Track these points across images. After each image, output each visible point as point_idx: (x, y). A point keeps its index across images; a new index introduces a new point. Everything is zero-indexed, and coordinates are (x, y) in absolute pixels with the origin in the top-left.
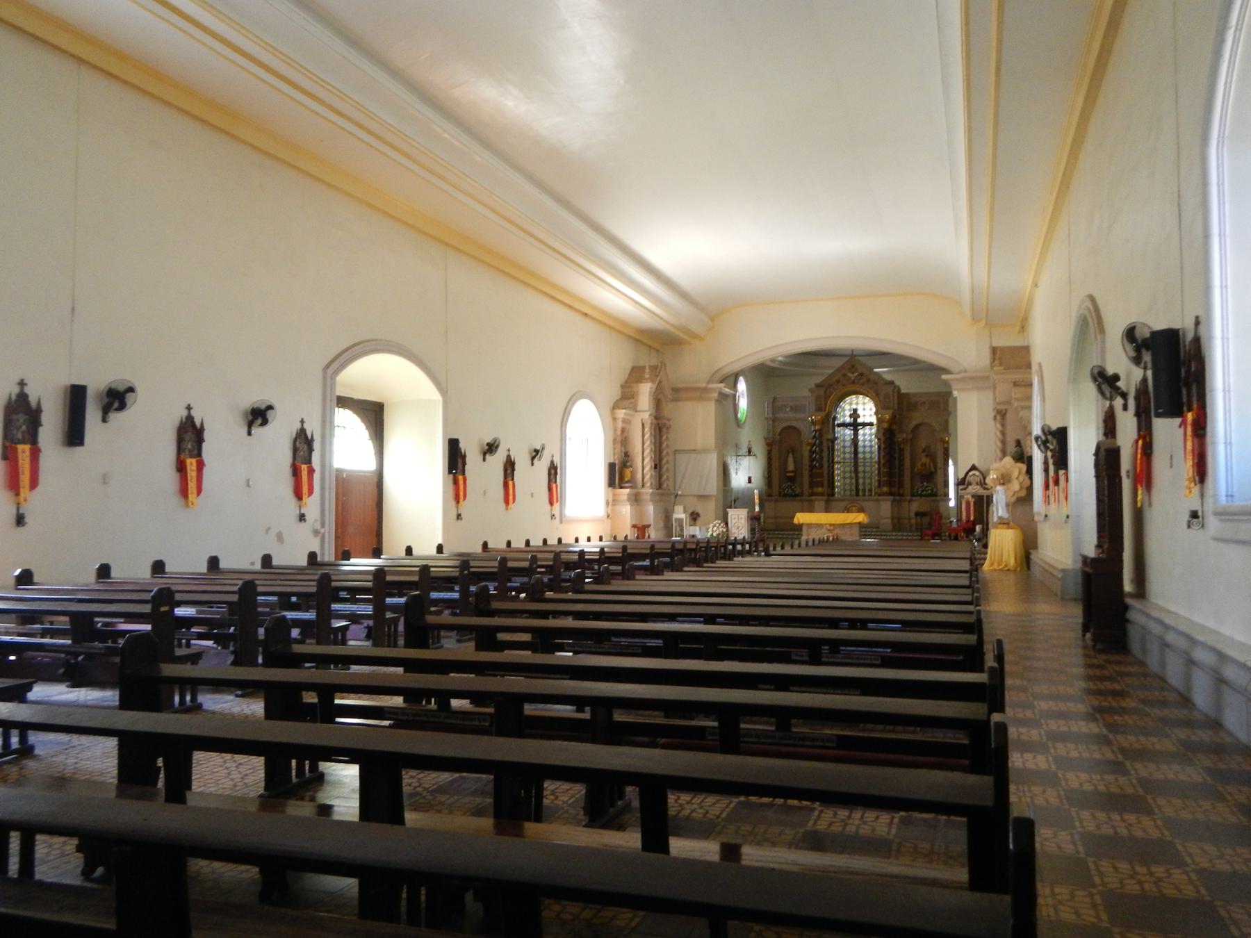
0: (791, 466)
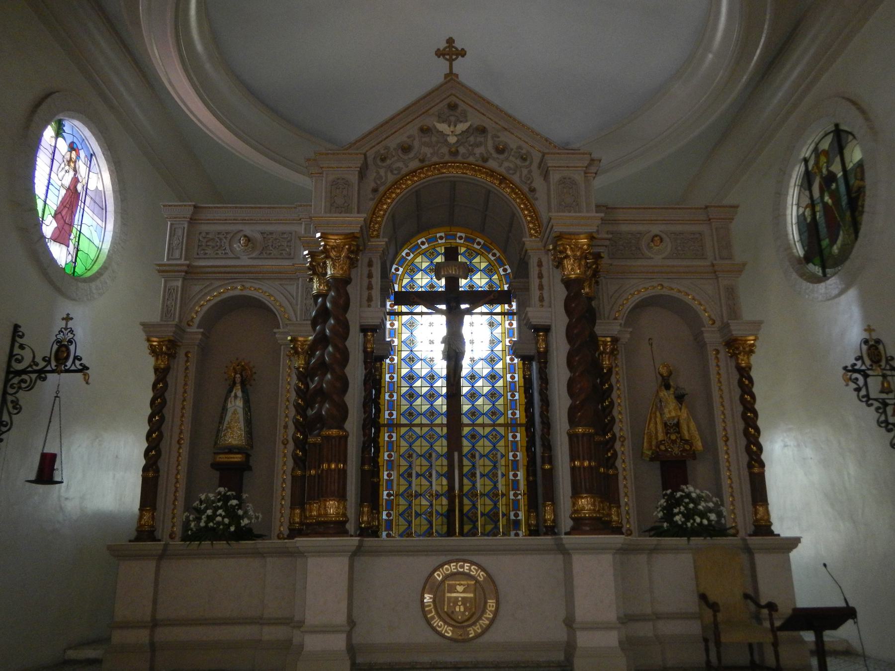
0: (235, 435)
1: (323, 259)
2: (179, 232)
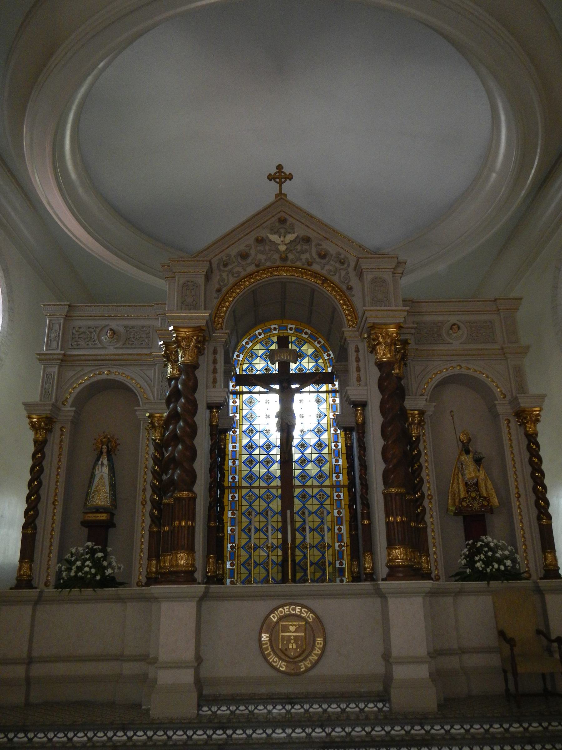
1: (175, 348)
2: (56, 327)
